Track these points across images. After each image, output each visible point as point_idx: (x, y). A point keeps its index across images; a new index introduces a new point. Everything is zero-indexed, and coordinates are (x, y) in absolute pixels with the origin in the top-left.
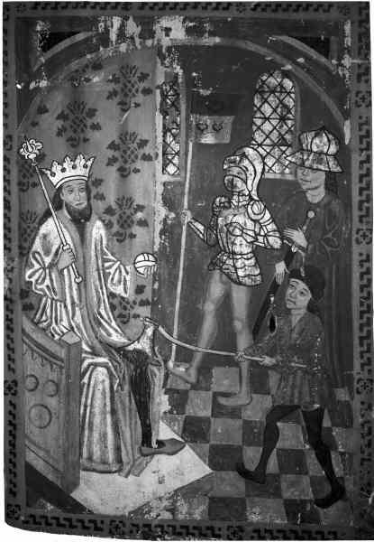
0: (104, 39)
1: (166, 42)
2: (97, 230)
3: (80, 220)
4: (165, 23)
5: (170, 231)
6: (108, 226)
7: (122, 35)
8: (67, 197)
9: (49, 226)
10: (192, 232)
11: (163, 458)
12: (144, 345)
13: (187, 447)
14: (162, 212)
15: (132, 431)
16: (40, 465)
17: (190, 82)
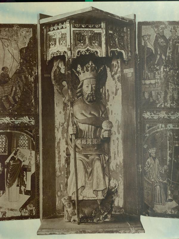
0: (158, 128)
1: (169, 128)
2: (157, 160)
3: (154, 159)
4: (169, 125)
5: (170, 161)
6: (159, 160)
7: (162, 127)
8: (151, 155)
9: (149, 160)
10: (174, 161)
11: (169, 203)
12: (165, 182)
13: (174, 202)
14: (168, 158)
15: (163, 197)
16: (147, 203)
17: (173, 135)
